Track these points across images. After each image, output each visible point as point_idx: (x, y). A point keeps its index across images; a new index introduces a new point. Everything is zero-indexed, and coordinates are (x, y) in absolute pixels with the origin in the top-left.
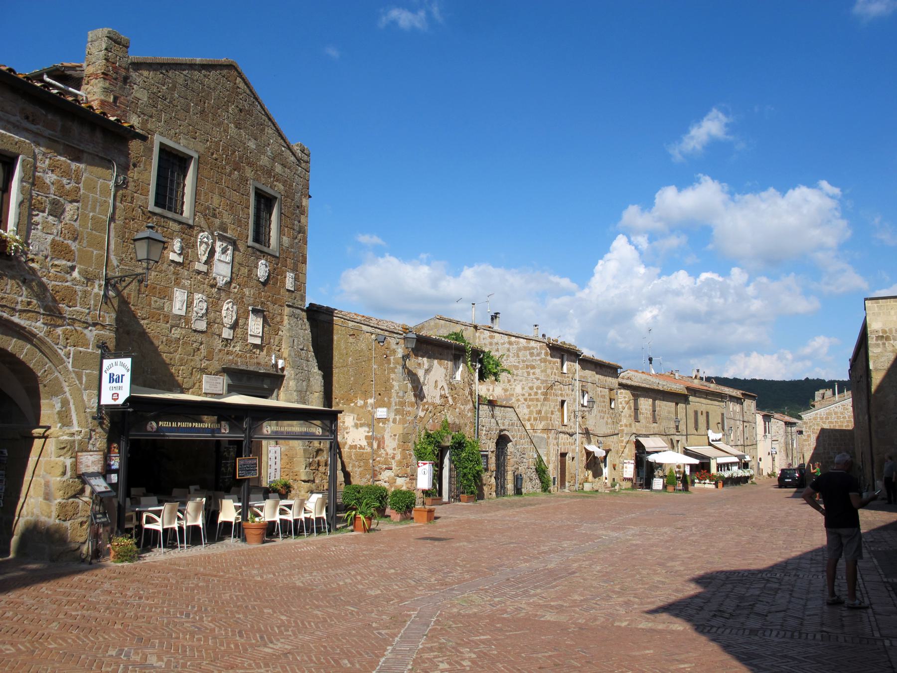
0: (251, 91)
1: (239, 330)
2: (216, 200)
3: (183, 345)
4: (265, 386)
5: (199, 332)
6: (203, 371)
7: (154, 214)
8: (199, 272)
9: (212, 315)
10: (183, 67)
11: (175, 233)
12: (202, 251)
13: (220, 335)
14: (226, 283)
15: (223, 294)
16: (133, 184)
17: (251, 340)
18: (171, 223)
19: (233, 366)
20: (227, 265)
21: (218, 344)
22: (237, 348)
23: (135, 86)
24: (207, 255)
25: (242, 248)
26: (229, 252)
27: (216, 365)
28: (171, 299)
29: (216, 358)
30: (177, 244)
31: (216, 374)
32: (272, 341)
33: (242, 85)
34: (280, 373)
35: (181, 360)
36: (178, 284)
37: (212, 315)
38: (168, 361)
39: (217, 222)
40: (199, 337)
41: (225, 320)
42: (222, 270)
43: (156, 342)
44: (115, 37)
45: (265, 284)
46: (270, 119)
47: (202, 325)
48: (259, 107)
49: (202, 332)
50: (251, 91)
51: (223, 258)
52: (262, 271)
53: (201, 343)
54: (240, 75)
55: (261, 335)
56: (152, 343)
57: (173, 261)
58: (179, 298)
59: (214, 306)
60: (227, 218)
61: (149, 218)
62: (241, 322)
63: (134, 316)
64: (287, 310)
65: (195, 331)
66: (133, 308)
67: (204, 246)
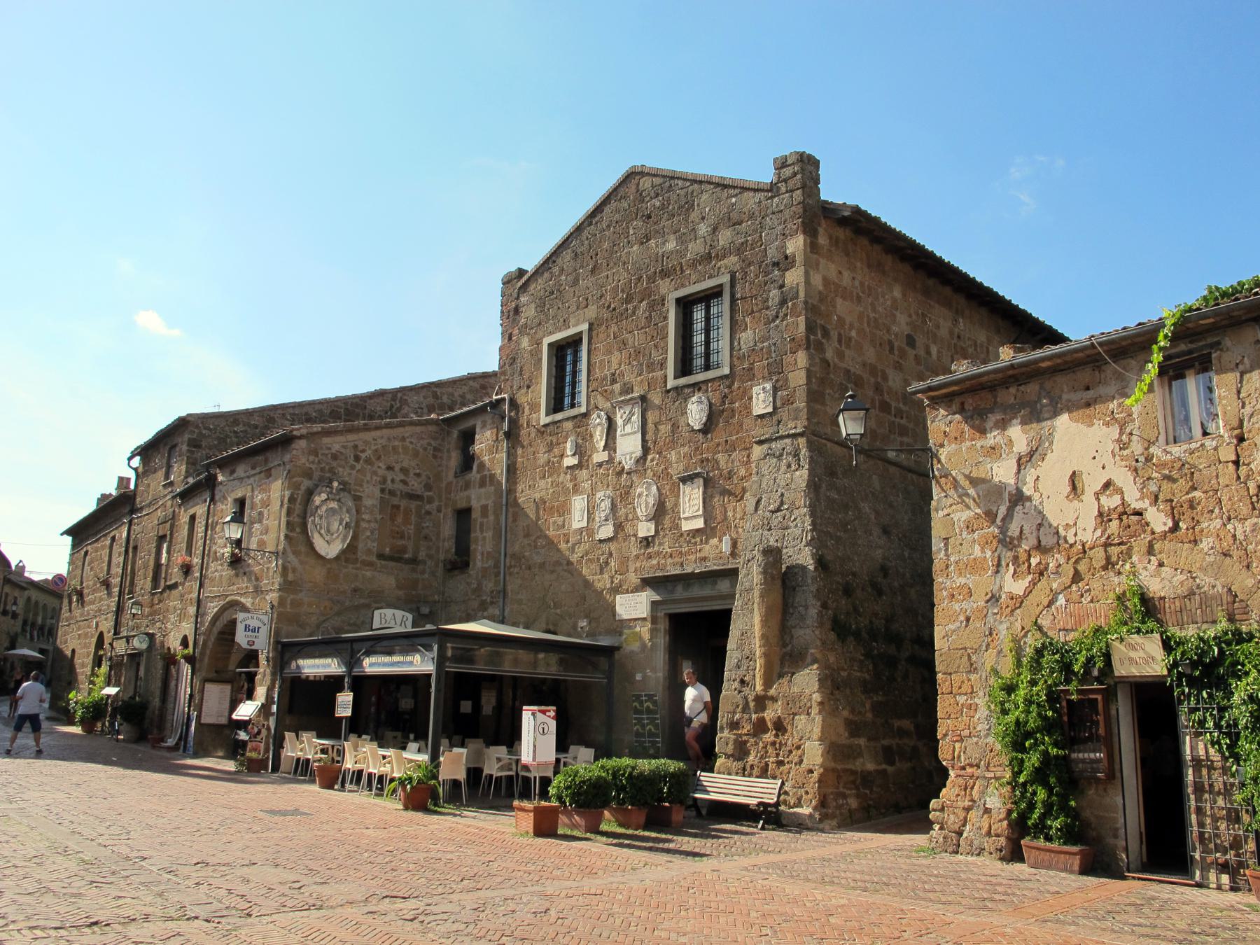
1: (667, 522)
8: (600, 465)
13: (635, 536)
14: (638, 461)
17: (686, 526)
25: (656, 398)
26: (634, 418)
27: (634, 579)
31: (636, 590)
32: (730, 514)
36: (576, 490)
39: (617, 387)
41: (639, 513)
42: (629, 445)
45: (706, 430)
48: (680, 183)
49: (610, 540)
52: (696, 413)
58: (578, 504)
59: (624, 496)
64: (757, 451)
65: (601, 541)
67: (599, 428)
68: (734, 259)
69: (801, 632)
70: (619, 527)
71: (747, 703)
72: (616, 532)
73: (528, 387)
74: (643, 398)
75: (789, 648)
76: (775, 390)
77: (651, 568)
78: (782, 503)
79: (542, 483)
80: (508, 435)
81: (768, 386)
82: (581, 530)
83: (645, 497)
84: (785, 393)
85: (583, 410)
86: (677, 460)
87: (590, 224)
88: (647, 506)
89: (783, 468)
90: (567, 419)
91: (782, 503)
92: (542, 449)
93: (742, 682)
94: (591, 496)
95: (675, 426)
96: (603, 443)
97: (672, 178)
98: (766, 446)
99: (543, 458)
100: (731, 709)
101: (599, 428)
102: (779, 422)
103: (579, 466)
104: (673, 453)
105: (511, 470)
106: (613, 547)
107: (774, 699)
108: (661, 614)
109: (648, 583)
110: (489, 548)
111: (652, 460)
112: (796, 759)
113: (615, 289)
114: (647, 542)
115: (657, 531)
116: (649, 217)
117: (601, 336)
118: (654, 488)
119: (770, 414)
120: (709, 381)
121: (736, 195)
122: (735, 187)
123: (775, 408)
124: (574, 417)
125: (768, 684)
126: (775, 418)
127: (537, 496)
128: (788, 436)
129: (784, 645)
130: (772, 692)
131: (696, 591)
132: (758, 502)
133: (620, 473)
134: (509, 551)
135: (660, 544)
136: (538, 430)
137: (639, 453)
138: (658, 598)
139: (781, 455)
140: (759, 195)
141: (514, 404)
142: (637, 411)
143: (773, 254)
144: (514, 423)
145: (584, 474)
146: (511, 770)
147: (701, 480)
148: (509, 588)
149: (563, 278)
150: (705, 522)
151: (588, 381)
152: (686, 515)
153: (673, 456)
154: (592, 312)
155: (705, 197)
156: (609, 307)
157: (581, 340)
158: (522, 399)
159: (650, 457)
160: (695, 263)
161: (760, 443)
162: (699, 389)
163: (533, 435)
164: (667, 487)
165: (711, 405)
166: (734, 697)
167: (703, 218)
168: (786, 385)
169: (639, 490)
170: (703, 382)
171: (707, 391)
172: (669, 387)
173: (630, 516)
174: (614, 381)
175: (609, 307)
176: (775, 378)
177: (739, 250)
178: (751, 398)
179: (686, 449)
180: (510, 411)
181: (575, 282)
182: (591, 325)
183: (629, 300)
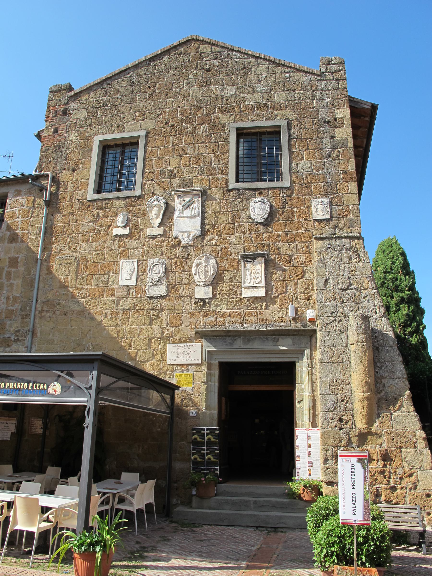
0: (222, 47)
1: (224, 287)
2: (173, 161)
3: (134, 315)
4: (282, 348)
5: (156, 297)
6: (170, 339)
7: (95, 201)
8: (153, 237)
9: (175, 277)
10: (127, 72)
11: (120, 209)
12: (155, 216)
13: (191, 297)
14: (195, 239)
15: (191, 251)
16: (72, 185)
17: (245, 293)
18: (114, 202)
19: (216, 328)
20: (193, 219)
21: (189, 307)
22: (224, 307)
23: (74, 113)
24: (161, 217)
25: (217, 194)
26: (195, 205)
27: (187, 331)
28: (116, 271)
29: (186, 322)
30: (120, 220)
31: (189, 340)
32: (291, 288)
33: (206, 48)
34: (310, 326)
35: (132, 331)
36: (125, 254)
37: (175, 277)
38: (114, 334)
39: (175, 181)
40: (158, 304)
41: (196, 278)
42: (187, 225)
43: (98, 317)
44: (55, 89)
45: (266, 223)
46: (257, 58)
47: (161, 290)
48: (238, 55)
49: (161, 297)
50: (222, 47)
51: (187, 213)
52: (258, 209)
53: (162, 310)
54: (203, 42)
55: (263, 284)
56: (94, 319)
57: (116, 236)
60: (189, 174)
61: (89, 206)
62: (226, 276)
63: (73, 296)
64: (317, 245)
65: (151, 298)
66: (71, 290)
67: (155, 210)
68: (288, 112)
69: (392, 382)
70: (172, 288)
71: (350, 438)
72: (168, 291)
73: (74, 170)
74: (204, 193)
75: (382, 394)
76: (331, 204)
77: (208, 323)
78: (350, 284)
79: (85, 246)
80: (48, 203)
81: (326, 201)
82: (129, 287)
83: (202, 268)
84: (340, 207)
85: (137, 193)
86: (237, 243)
87: (148, 65)
88: (206, 274)
89: (345, 260)
90: (119, 198)
91: (350, 284)
92: (87, 218)
93: (341, 420)
94: (142, 260)
95: (236, 217)
96: (159, 220)
97: (232, 50)
98: (326, 242)
99: (86, 226)
100: (336, 443)
101: (155, 210)
102: (336, 227)
103: (130, 236)
104: (233, 237)
105: (49, 232)
106: (165, 303)
107: (378, 435)
108: (215, 363)
109: (203, 335)
110: (16, 293)
111: (211, 240)
112: (410, 486)
113: (174, 114)
114: (203, 302)
115: (214, 295)
116: (208, 70)
117: (158, 143)
118: (212, 261)
119: (327, 220)
120: (271, 189)
121: (289, 73)
122: (288, 67)
123: (332, 217)
124: (125, 198)
125: (370, 422)
126: (332, 224)
127: (79, 255)
128: (347, 237)
129: (379, 392)
130: (375, 428)
131: (257, 345)
132: (326, 281)
133: (174, 247)
134: (42, 298)
135: (217, 306)
136: (83, 204)
137: (198, 232)
138: (212, 348)
139: (341, 250)
140: (309, 77)
141: (55, 180)
142: (197, 201)
143: (323, 114)
144: (54, 196)
145: (135, 242)
146: (108, 503)
147: (263, 260)
148: (38, 329)
149: (119, 96)
150: (266, 293)
151: (144, 172)
152: (245, 285)
153: (233, 239)
154: (149, 124)
155: (260, 68)
156: (167, 123)
157: (137, 143)
158: (64, 177)
159: (208, 237)
160: (252, 108)
161: (321, 239)
162: (260, 194)
163: (76, 207)
164: (226, 262)
165: (271, 206)
166: (335, 433)
167: (260, 81)
168: (340, 202)
169: (196, 262)
170: (265, 189)
171: (268, 195)
172: (230, 187)
173: (186, 281)
174: (172, 176)
175: (167, 123)
176: (331, 196)
177: (294, 107)
178: (309, 207)
179: (247, 235)
180: (51, 186)
181: (132, 101)
182: (147, 133)
183: (189, 121)
